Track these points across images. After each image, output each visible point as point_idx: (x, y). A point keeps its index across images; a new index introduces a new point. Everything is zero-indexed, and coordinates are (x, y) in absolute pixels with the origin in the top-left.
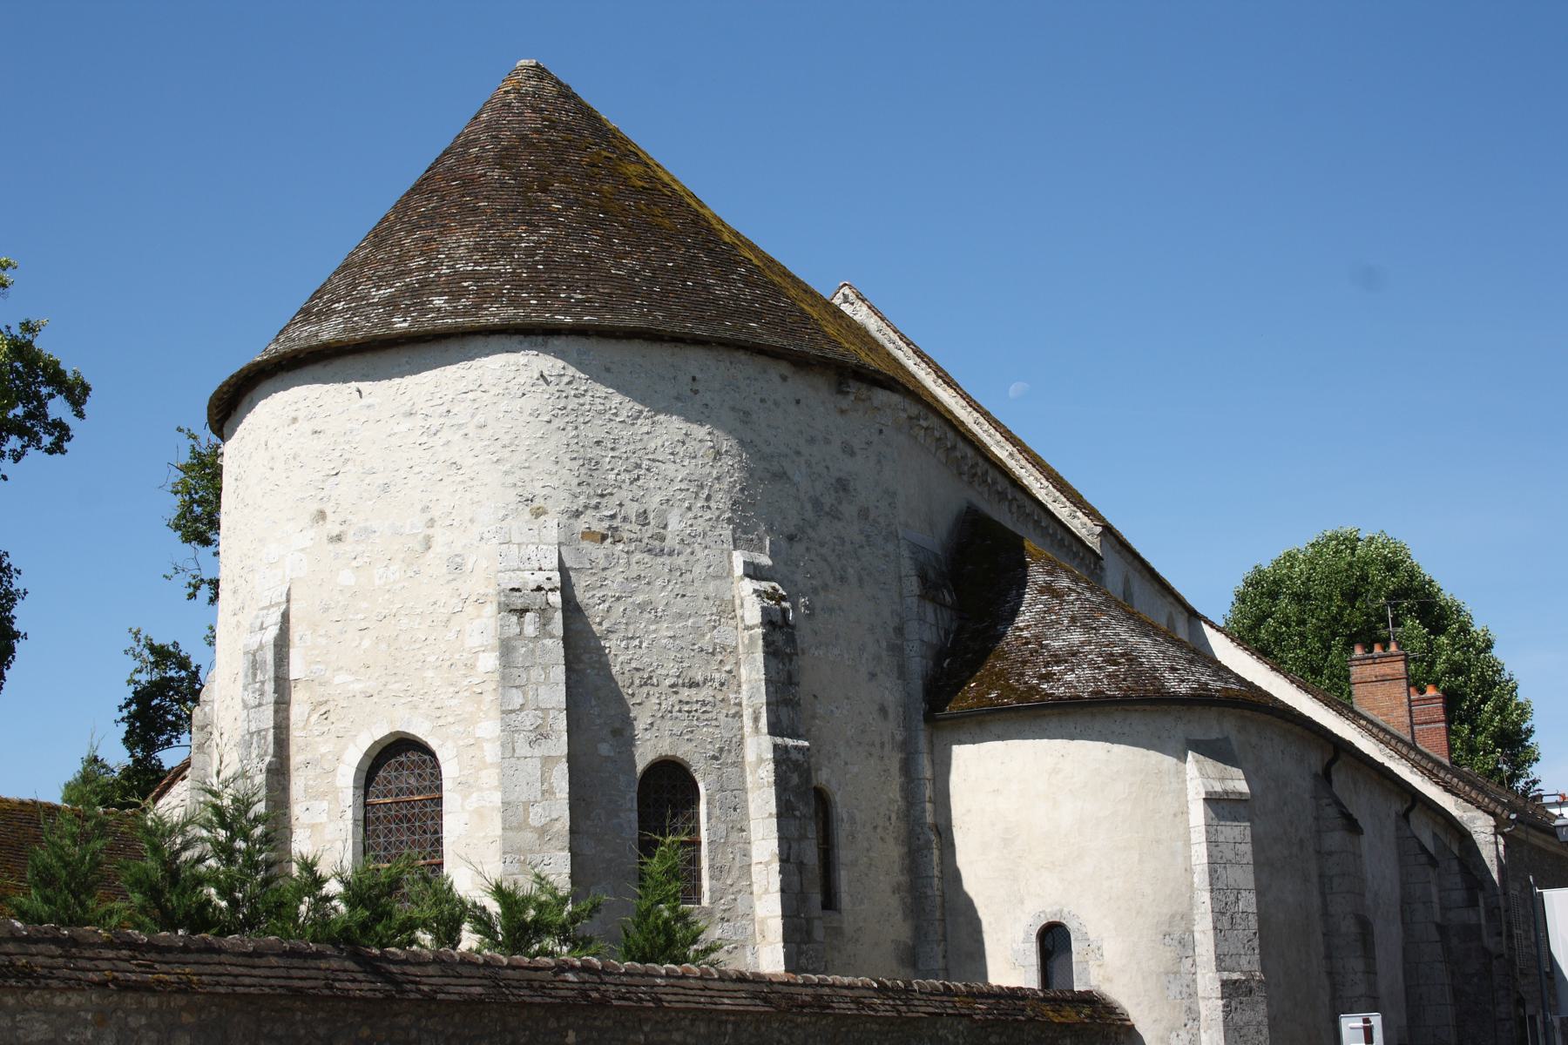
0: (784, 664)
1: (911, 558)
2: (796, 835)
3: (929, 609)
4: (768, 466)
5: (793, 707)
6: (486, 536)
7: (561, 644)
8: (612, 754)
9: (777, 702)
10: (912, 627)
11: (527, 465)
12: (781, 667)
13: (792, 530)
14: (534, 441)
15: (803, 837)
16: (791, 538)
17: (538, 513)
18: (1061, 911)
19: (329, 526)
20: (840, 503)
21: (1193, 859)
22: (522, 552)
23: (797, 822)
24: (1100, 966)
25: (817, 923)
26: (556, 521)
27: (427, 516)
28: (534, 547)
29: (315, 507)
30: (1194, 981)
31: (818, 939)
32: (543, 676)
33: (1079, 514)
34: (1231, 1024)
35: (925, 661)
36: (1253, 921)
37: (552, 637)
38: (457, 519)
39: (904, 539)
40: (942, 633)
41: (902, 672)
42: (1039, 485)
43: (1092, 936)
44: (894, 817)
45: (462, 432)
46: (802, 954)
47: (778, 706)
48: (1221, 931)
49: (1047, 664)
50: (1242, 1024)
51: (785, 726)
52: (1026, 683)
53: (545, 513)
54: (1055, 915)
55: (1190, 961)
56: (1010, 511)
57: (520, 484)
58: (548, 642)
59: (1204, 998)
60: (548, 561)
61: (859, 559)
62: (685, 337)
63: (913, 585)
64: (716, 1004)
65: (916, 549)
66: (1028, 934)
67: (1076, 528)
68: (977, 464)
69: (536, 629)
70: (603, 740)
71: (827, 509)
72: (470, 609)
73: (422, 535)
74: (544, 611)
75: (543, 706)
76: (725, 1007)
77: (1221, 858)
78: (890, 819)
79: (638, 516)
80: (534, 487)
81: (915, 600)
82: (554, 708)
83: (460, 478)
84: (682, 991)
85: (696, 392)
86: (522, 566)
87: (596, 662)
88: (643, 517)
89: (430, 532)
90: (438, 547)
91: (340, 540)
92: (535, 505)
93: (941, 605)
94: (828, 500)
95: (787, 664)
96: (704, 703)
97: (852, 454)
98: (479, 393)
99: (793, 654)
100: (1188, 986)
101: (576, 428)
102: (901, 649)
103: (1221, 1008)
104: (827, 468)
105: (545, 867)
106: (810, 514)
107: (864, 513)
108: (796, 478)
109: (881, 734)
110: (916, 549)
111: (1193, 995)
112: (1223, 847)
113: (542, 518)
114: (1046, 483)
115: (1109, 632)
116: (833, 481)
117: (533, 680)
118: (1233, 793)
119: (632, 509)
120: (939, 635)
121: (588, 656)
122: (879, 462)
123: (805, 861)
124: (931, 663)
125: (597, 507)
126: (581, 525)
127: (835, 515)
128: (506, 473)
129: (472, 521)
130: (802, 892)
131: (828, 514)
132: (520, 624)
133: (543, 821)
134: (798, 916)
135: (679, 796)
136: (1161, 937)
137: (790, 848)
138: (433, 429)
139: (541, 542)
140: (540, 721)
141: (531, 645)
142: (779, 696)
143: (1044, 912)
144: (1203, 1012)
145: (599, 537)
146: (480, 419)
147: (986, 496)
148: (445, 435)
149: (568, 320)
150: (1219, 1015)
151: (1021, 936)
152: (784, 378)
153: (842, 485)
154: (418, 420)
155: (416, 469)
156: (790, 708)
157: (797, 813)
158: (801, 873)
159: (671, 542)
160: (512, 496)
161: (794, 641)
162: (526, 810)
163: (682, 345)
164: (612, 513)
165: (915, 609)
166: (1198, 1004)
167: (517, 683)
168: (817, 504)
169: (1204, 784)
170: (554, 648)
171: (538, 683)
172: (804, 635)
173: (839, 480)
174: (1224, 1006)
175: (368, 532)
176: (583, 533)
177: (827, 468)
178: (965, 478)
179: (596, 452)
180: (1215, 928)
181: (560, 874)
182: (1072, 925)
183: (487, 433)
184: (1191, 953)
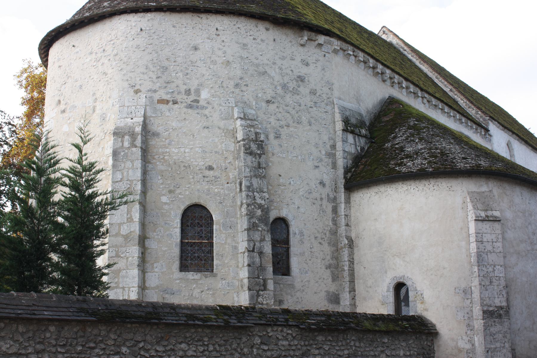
0: (256, 158)
1: (339, 113)
2: (259, 239)
3: (350, 138)
4: (256, 69)
5: (260, 179)
6: (115, 103)
7: (140, 150)
8: (168, 201)
9: (251, 176)
10: (339, 145)
11: (133, 70)
12: (254, 159)
13: (269, 98)
14: (137, 60)
15: (262, 240)
16: (268, 102)
17: (137, 92)
18: (404, 276)
19: (61, 107)
20: (299, 87)
21: (471, 250)
22: (129, 110)
23: (259, 233)
24: (422, 303)
25: (269, 281)
26: (145, 95)
27: (95, 97)
28: (133, 108)
29: (57, 99)
30: (472, 311)
31: (270, 289)
32: (131, 165)
33: (480, 113)
34: (488, 332)
35: (346, 160)
36: (503, 281)
37: (136, 147)
38: (105, 97)
39: (337, 104)
40: (359, 148)
41: (334, 166)
42: (462, 102)
43: (418, 289)
44: (328, 233)
45: (108, 58)
46: (259, 296)
47: (251, 178)
48: (484, 286)
49: (402, 158)
50: (494, 332)
51: (255, 188)
52: (390, 167)
53: (140, 91)
54: (401, 278)
55: (469, 301)
56: (423, 103)
57: (130, 79)
58: (134, 149)
59: (476, 319)
60: (139, 113)
61: (309, 113)
62: (211, 9)
63: (339, 126)
64: (34, 314)
65: (343, 110)
66: (388, 287)
67: (478, 118)
68: (395, 77)
69: (129, 143)
70: (164, 195)
71: (291, 89)
72: (107, 137)
73: (92, 106)
74: (133, 135)
75: (130, 179)
76: (45, 317)
77: (485, 249)
78: (325, 234)
79: (186, 92)
80: (136, 80)
81: (341, 132)
82: (135, 180)
83: (106, 79)
84: (5, 306)
85: (218, 35)
86: (128, 116)
87: (162, 159)
88: (188, 92)
89: (95, 104)
90: (98, 111)
91: (64, 112)
92: (136, 88)
93: (358, 135)
94: (292, 85)
95: (258, 158)
96: (215, 177)
97: (307, 65)
98: (115, 41)
99: (262, 154)
100: (468, 313)
101: (157, 52)
102: (335, 155)
103: (483, 324)
104: (292, 71)
105: (127, 254)
106: (280, 90)
107: (313, 92)
108: (273, 74)
109: (321, 194)
110: (343, 110)
111: (471, 318)
112: (485, 244)
113: (139, 94)
114: (465, 101)
115: (437, 144)
116: (296, 77)
117: (126, 167)
118: (491, 216)
119: (183, 88)
120: (356, 148)
121: (158, 156)
122: (323, 69)
123: (264, 251)
124: (351, 162)
125: (166, 87)
126: (157, 97)
127: (295, 92)
128: (124, 75)
129: (109, 97)
130: (261, 266)
131: (291, 91)
132: (122, 142)
133: (127, 233)
134: (258, 278)
135: (203, 221)
136: (454, 289)
137: (255, 245)
138: (98, 59)
139: (138, 105)
140: (129, 186)
141: (126, 151)
142: (252, 173)
143: (396, 277)
144: (476, 327)
145: (166, 102)
146: (115, 52)
147: (405, 94)
148: (101, 61)
149: (154, 4)
150: (482, 328)
151: (385, 289)
152: (267, 29)
153: (301, 79)
154: (94, 56)
155: (92, 77)
156: (259, 179)
157: (260, 229)
158: (260, 258)
159: (202, 103)
160: (126, 84)
161: (262, 148)
162: (120, 228)
163: (211, 14)
164: (172, 91)
165: (341, 136)
166: (473, 322)
167: (120, 169)
168: (284, 87)
169: (475, 213)
170: (137, 152)
171: (128, 169)
172: (273, 145)
173: (299, 77)
174: (484, 323)
175: (74, 107)
176: (158, 100)
177: (292, 71)
178: (388, 82)
179: (166, 63)
180: (480, 284)
181: (133, 257)
182: (408, 283)
183: (117, 58)
184: (470, 297)
